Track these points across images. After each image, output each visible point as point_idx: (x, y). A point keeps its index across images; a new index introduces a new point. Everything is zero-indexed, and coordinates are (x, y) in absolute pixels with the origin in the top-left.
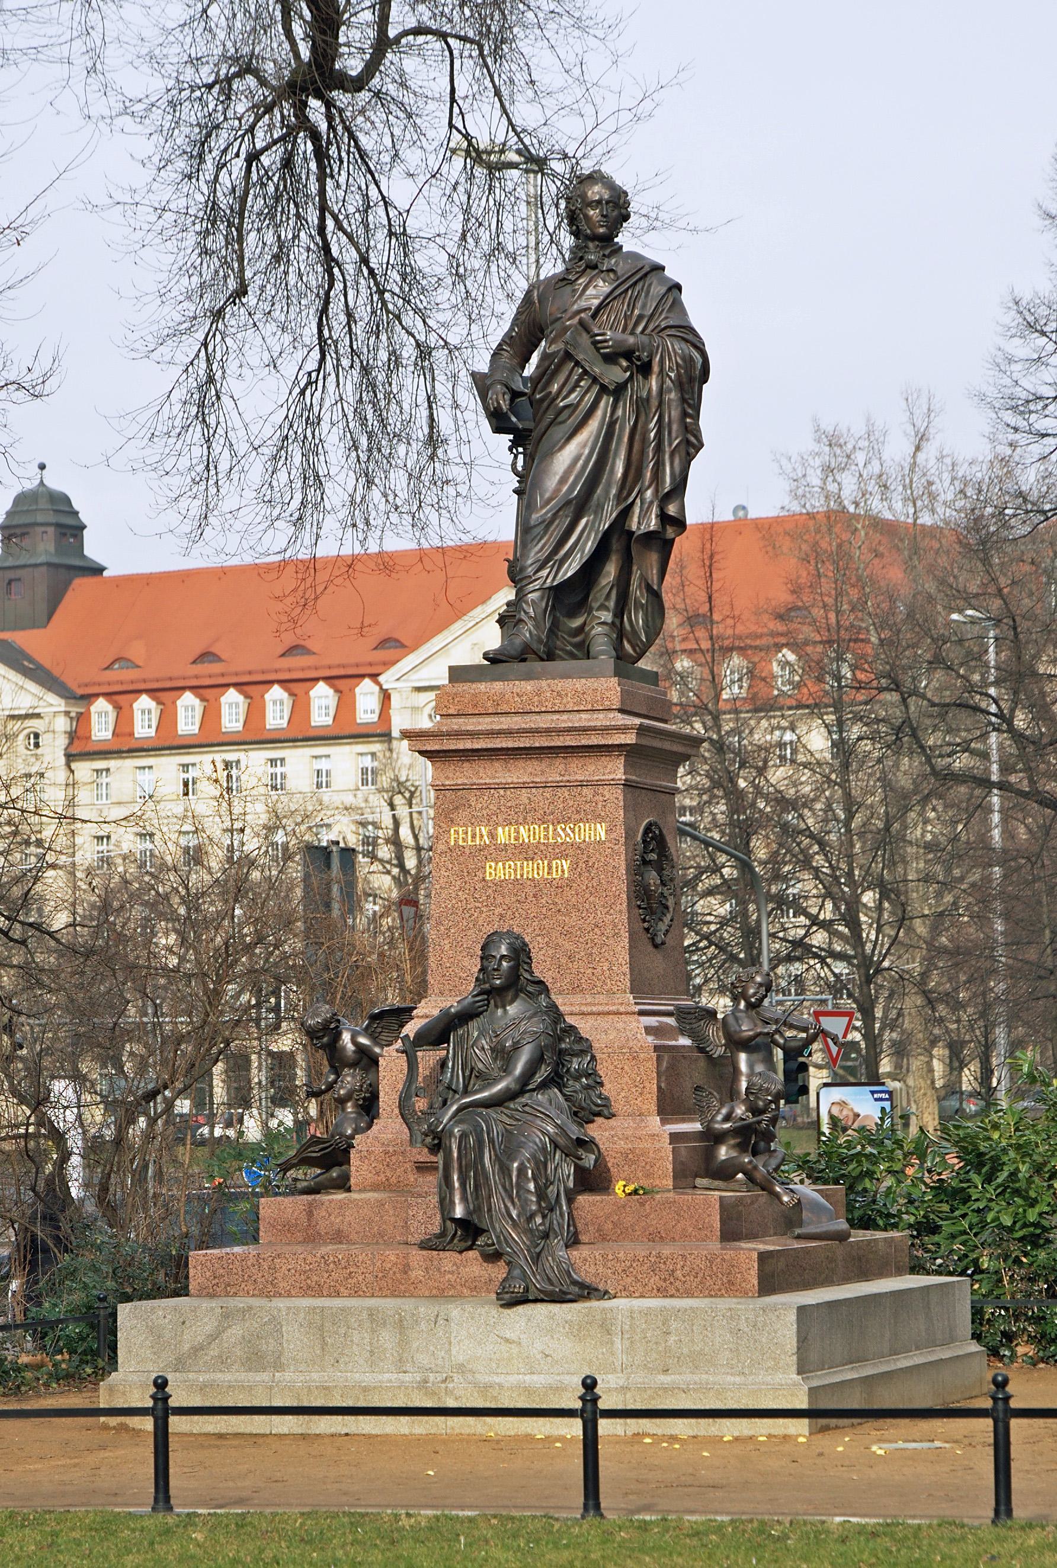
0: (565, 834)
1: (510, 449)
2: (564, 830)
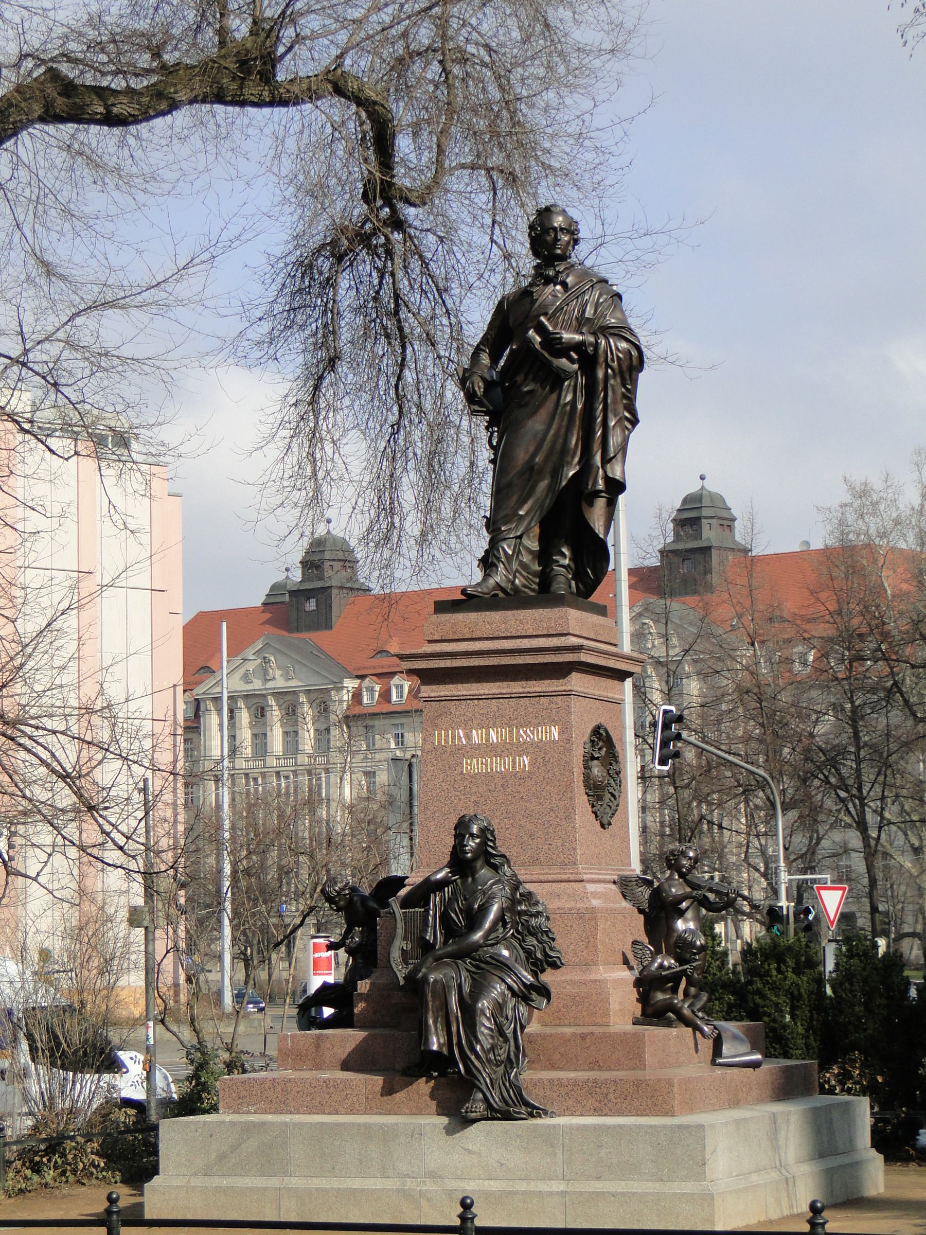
0: (527, 735)
1: (487, 428)
2: (525, 732)
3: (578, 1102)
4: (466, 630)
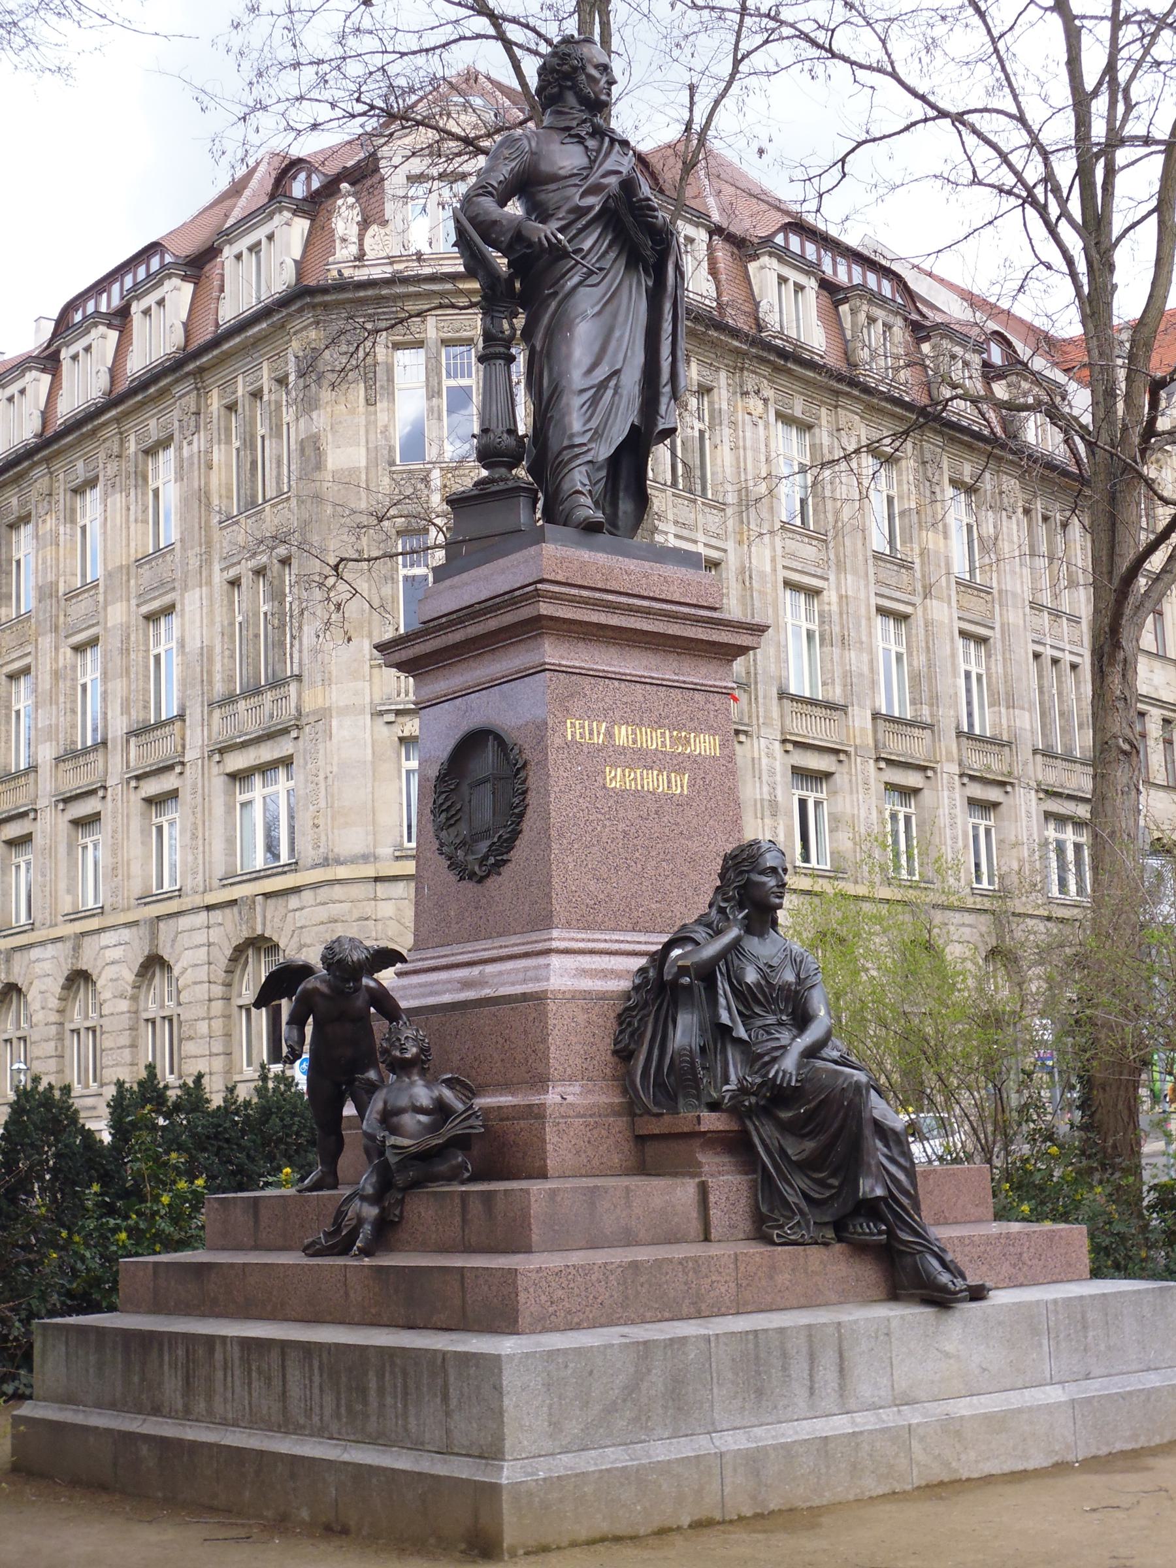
3: (991, 1268)
4: (599, 576)
